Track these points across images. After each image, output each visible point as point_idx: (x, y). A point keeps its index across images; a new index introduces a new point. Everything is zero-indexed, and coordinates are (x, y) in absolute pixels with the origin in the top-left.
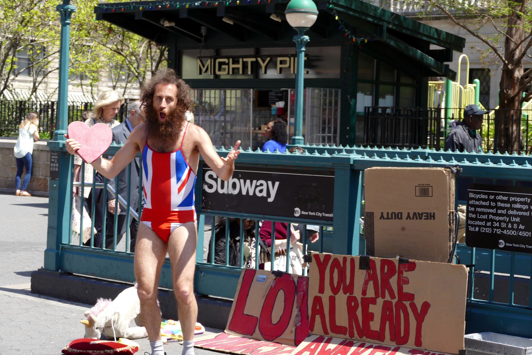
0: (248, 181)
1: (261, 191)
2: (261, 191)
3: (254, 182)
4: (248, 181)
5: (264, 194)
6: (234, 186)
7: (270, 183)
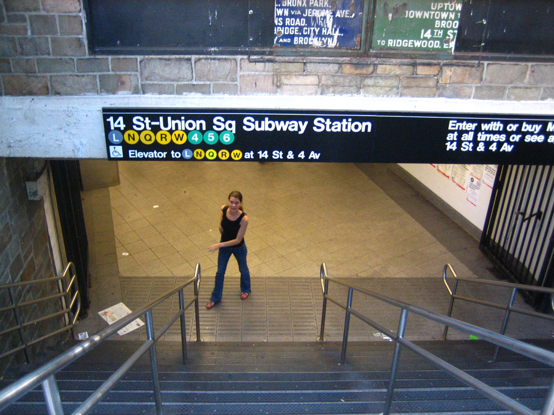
0: (282, 122)
1: (293, 128)
2: (293, 128)
3: (287, 123)
4: (282, 122)
5: (296, 129)
6: (270, 126)
7: (300, 123)
